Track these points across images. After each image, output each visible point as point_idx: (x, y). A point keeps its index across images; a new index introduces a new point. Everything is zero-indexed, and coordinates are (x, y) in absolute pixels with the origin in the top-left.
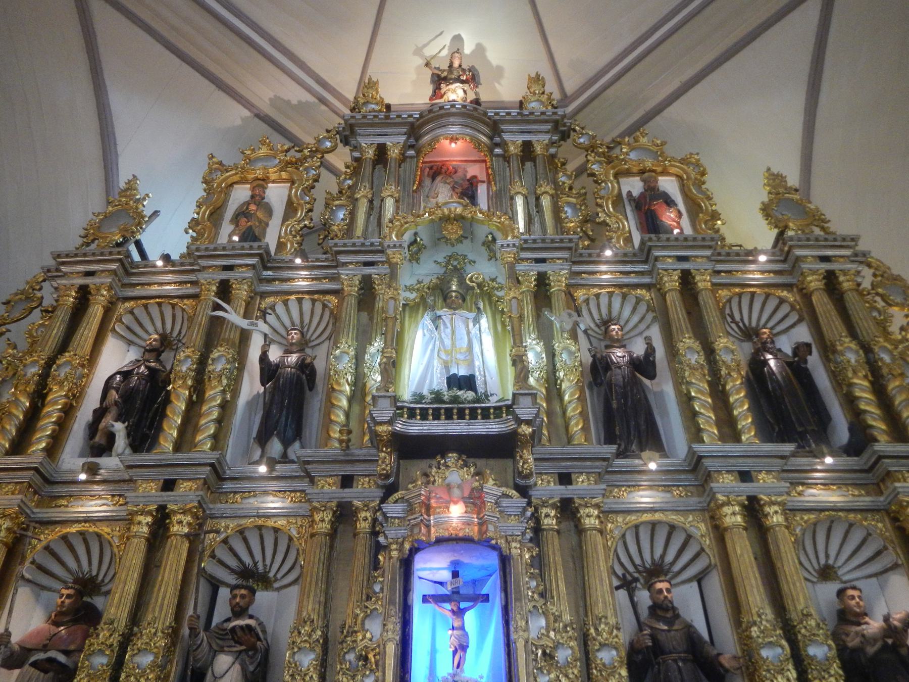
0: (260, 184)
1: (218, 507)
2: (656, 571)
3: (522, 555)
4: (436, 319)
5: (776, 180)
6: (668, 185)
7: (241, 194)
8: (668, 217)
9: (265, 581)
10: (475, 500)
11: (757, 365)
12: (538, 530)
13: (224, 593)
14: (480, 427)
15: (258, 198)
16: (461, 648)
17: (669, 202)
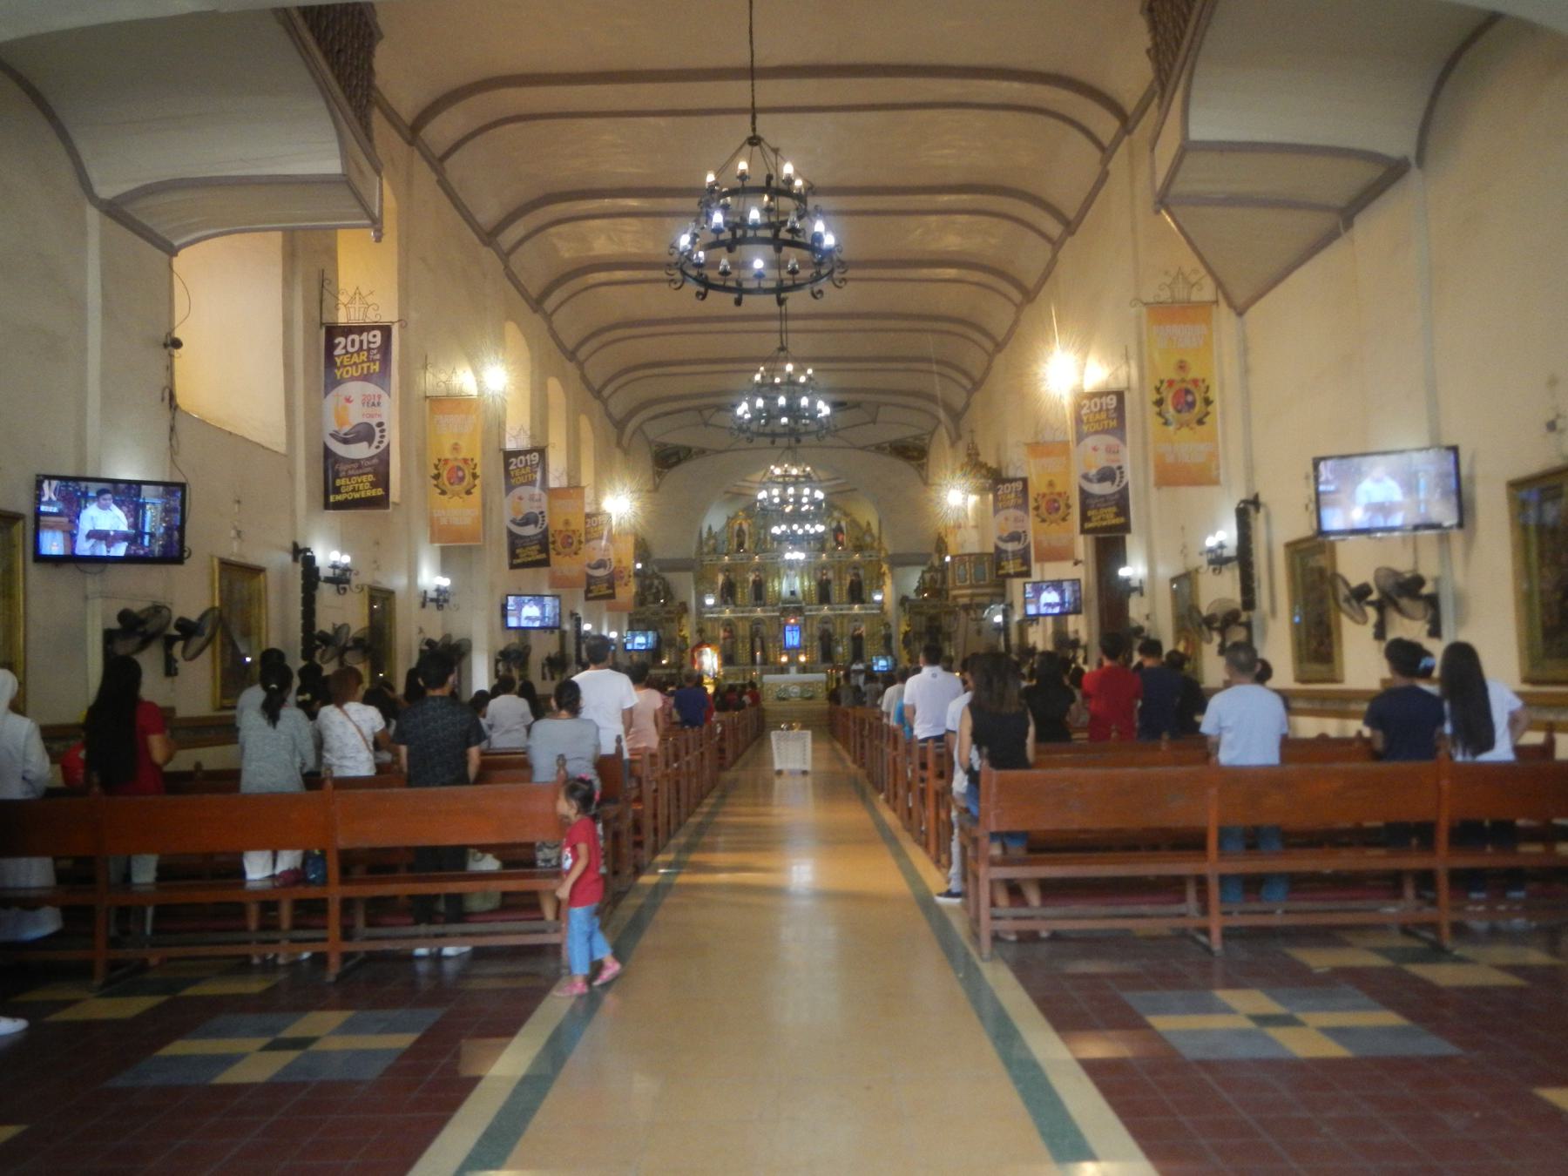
0: (741, 525)
1: (752, 615)
2: (826, 623)
3: (803, 630)
4: (787, 576)
5: (869, 524)
6: (843, 524)
7: (736, 527)
8: (840, 538)
9: (759, 624)
10: (795, 618)
11: (852, 582)
12: (805, 620)
13: (754, 627)
14: (796, 605)
15: (741, 531)
16: (793, 638)
17: (842, 532)
